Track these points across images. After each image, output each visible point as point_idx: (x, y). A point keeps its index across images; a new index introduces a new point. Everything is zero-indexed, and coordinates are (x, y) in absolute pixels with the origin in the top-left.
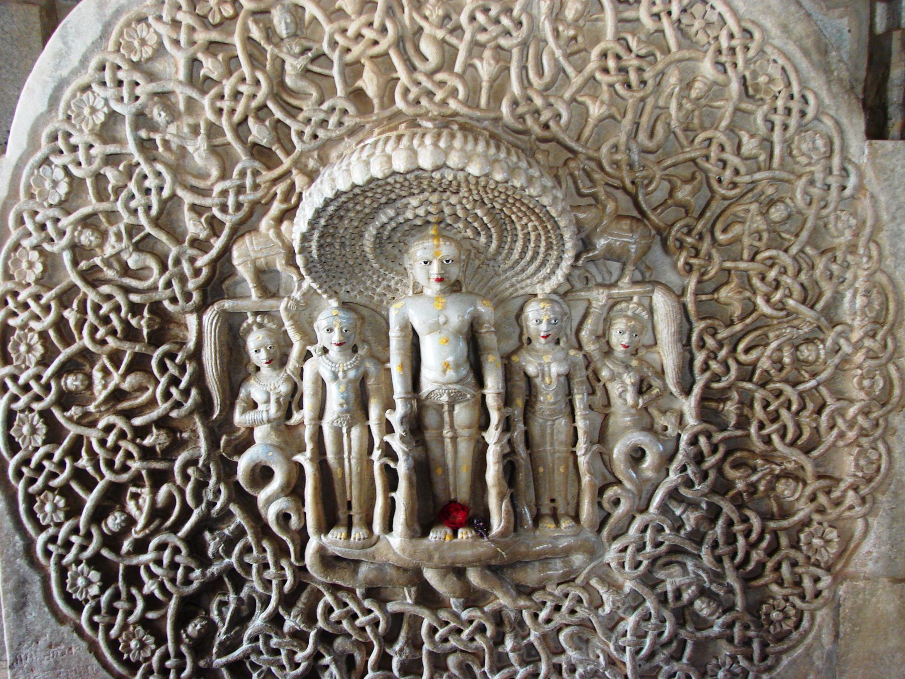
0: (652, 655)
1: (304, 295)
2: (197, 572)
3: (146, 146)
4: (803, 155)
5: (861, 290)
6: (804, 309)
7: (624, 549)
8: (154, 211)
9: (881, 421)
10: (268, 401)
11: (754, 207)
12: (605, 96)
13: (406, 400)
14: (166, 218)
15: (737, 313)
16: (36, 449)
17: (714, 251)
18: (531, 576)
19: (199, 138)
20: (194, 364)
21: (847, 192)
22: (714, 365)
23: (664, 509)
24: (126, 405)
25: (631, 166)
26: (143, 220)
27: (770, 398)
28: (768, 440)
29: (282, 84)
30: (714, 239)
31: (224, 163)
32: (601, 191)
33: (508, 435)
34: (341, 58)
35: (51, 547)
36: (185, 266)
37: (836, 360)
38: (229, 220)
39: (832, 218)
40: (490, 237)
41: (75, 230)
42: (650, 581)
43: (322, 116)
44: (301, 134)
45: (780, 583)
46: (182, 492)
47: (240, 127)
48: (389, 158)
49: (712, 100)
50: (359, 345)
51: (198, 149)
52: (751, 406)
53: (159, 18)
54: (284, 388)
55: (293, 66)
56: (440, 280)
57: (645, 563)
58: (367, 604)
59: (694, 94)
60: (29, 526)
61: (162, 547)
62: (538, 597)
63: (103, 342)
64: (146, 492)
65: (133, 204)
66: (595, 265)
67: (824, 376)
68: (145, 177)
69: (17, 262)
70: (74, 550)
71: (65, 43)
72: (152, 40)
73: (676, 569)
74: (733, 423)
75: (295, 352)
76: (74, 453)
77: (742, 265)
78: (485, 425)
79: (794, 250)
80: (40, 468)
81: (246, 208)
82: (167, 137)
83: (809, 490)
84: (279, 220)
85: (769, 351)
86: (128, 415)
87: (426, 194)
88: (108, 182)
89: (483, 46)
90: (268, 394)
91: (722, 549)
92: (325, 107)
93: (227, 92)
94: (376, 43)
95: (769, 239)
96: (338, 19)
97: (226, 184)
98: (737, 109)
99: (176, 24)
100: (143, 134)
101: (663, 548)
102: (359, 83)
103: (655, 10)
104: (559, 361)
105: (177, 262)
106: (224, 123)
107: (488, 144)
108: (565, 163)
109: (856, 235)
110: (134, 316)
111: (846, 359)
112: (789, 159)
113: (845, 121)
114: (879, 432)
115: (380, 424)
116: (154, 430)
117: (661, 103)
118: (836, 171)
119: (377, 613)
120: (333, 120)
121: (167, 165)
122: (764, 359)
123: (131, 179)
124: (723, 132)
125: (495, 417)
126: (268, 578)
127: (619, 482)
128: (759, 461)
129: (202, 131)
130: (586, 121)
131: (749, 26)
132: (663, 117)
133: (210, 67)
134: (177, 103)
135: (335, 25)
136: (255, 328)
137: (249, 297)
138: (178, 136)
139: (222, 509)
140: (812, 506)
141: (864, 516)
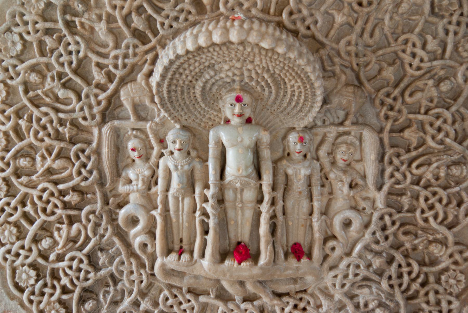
1: (161, 120)
2: (92, 275)
3: (69, 25)
6: (456, 145)
7: (336, 276)
8: (74, 65)
10: (137, 180)
11: (431, 82)
12: (346, 10)
13: (215, 185)
14: (80, 70)
15: (414, 145)
17: (403, 107)
19: (102, 22)
20: (96, 156)
22: (397, 175)
24: (55, 177)
25: (357, 55)
26: (67, 69)
28: (426, 220)
30: (403, 102)
31: (117, 39)
32: (337, 69)
33: (274, 208)
35: (7, 256)
36: (92, 98)
38: (119, 73)
41: (26, 72)
43: (175, 14)
44: (163, 24)
45: (428, 303)
46: (86, 229)
47: (127, 19)
48: (211, 33)
49: (410, 15)
54: (147, 173)
56: (240, 115)
58: (188, 296)
59: (400, 11)
61: (72, 259)
62: (285, 299)
63: (42, 140)
64: (64, 227)
68: (69, 44)
70: (21, 258)
73: (366, 290)
75: (155, 152)
77: (420, 117)
78: (260, 201)
81: (128, 67)
82: (83, 20)
83: (449, 251)
86: (56, 183)
88: (47, 45)
90: (138, 175)
91: (394, 282)
92: (178, 8)
95: (438, 102)
98: (426, 21)
100: (68, 17)
101: (359, 278)
104: (307, 167)
105: (87, 96)
106: (117, 14)
107: (275, 29)
112: (455, 54)
115: (200, 198)
116: (71, 192)
117: (380, 16)
119: (193, 302)
120: (182, 17)
121: (82, 36)
122: (428, 173)
123: (60, 44)
125: (267, 198)
128: (420, 232)
129: (104, 18)
130: (332, 26)
132: (380, 25)
136: (132, 137)
137: (128, 118)
138: (89, 19)
139: (108, 240)
140: (451, 260)
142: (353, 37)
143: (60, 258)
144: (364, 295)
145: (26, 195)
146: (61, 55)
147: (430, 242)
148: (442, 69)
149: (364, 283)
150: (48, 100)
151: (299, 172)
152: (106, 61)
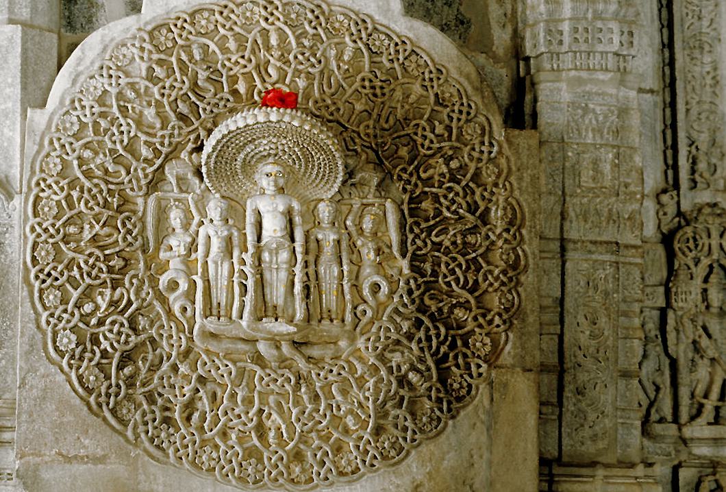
0: (384, 403)
2: (133, 338)
3: (123, 110)
4: (469, 134)
5: (501, 206)
6: (467, 215)
8: (125, 143)
9: (514, 278)
11: (441, 160)
12: (363, 101)
14: (130, 148)
15: (432, 215)
16: (48, 264)
17: (419, 182)
18: (315, 352)
21: (493, 155)
23: (391, 319)
25: (375, 136)
26: (119, 147)
27: (450, 262)
28: (448, 284)
29: (196, 84)
30: (419, 177)
33: (307, 270)
34: (227, 72)
35: (51, 319)
37: (487, 243)
38: (165, 150)
39: (484, 167)
40: (300, 165)
41: (81, 149)
42: (381, 358)
43: (217, 101)
45: (458, 366)
50: (230, 220)
51: (150, 114)
52: (440, 266)
53: (133, 45)
54: (189, 240)
55: (202, 75)
57: (380, 347)
60: (39, 306)
63: (92, 209)
64: (108, 292)
65: (114, 138)
66: (356, 188)
67: (480, 251)
68: (121, 125)
69: (47, 164)
70: (63, 322)
71: (83, 53)
72: (129, 56)
73: (398, 354)
74: (429, 273)
76: (69, 267)
77: (434, 190)
79: (464, 183)
80: (49, 275)
83: (473, 314)
84: (191, 153)
85: (449, 236)
87: (271, 137)
89: (300, 72)
91: (424, 344)
92: (217, 97)
93: (167, 85)
94: (246, 67)
96: (227, 53)
97: (165, 132)
98: (433, 110)
99: (142, 49)
100: (122, 103)
101: (390, 341)
102: (236, 86)
103: (390, 57)
104: (335, 233)
105: (136, 170)
108: (341, 133)
109: (498, 176)
110: (110, 196)
111: (493, 243)
113: (491, 118)
114: (513, 284)
118: (487, 144)
119: (230, 366)
122: (446, 240)
124: (425, 121)
126: (171, 346)
127: (365, 302)
128: (445, 297)
131: (440, 68)
133: (159, 72)
134: (140, 89)
135: (225, 56)
136: (174, 207)
141: (505, 331)
142: (371, 123)
143: (101, 323)
144: (396, 358)
145: (74, 259)
146: (114, 135)
147: (454, 306)
148: (450, 149)
149: (397, 347)
150: (99, 173)
151: (328, 237)
152: (154, 140)
